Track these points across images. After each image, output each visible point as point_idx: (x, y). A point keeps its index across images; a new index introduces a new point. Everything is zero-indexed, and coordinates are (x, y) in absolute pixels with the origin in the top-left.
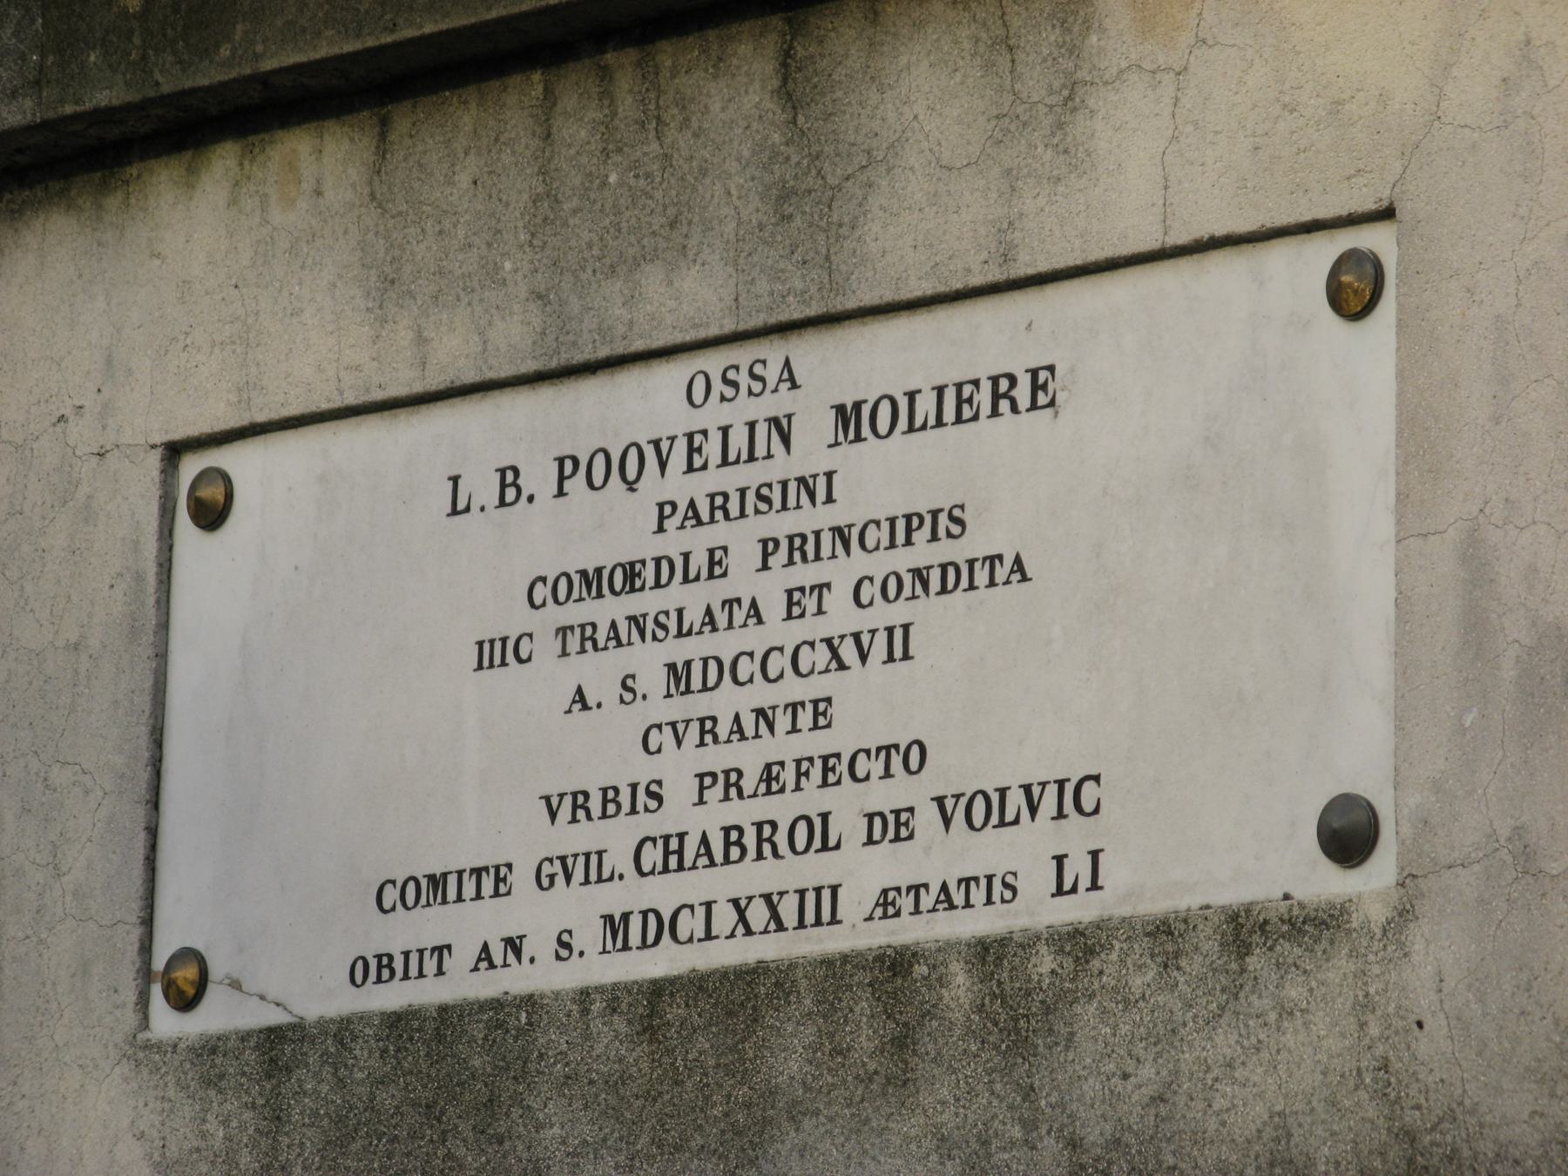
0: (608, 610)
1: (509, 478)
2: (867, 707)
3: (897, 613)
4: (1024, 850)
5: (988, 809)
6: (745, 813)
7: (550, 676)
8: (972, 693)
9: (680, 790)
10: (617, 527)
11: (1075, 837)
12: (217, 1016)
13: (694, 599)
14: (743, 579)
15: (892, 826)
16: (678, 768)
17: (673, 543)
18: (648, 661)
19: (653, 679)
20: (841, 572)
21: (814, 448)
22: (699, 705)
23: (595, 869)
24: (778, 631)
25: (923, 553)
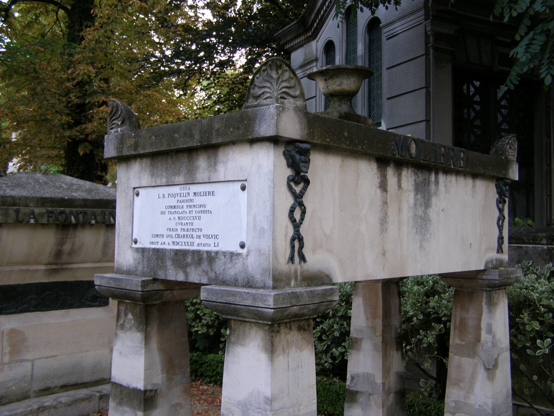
0: (173, 210)
1: (164, 195)
2: (197, 224)
3: (199, 215)
4: (211, 241)
5: (207, 237)
6: (186, 233)
7: (167, 216)
9: (179, 230)
11: (216, 241)
12: (138, 245)
14: (185, 209)
15: (199, 237)
16: (179, 227)
17: (179, 204)
18: (176, 216)
19: (177, 218)
20: (194, 210)
21: (191, 196)
22: (181, 221)
23: (171, 236)
24: (188, 215)
25: (202, 209)
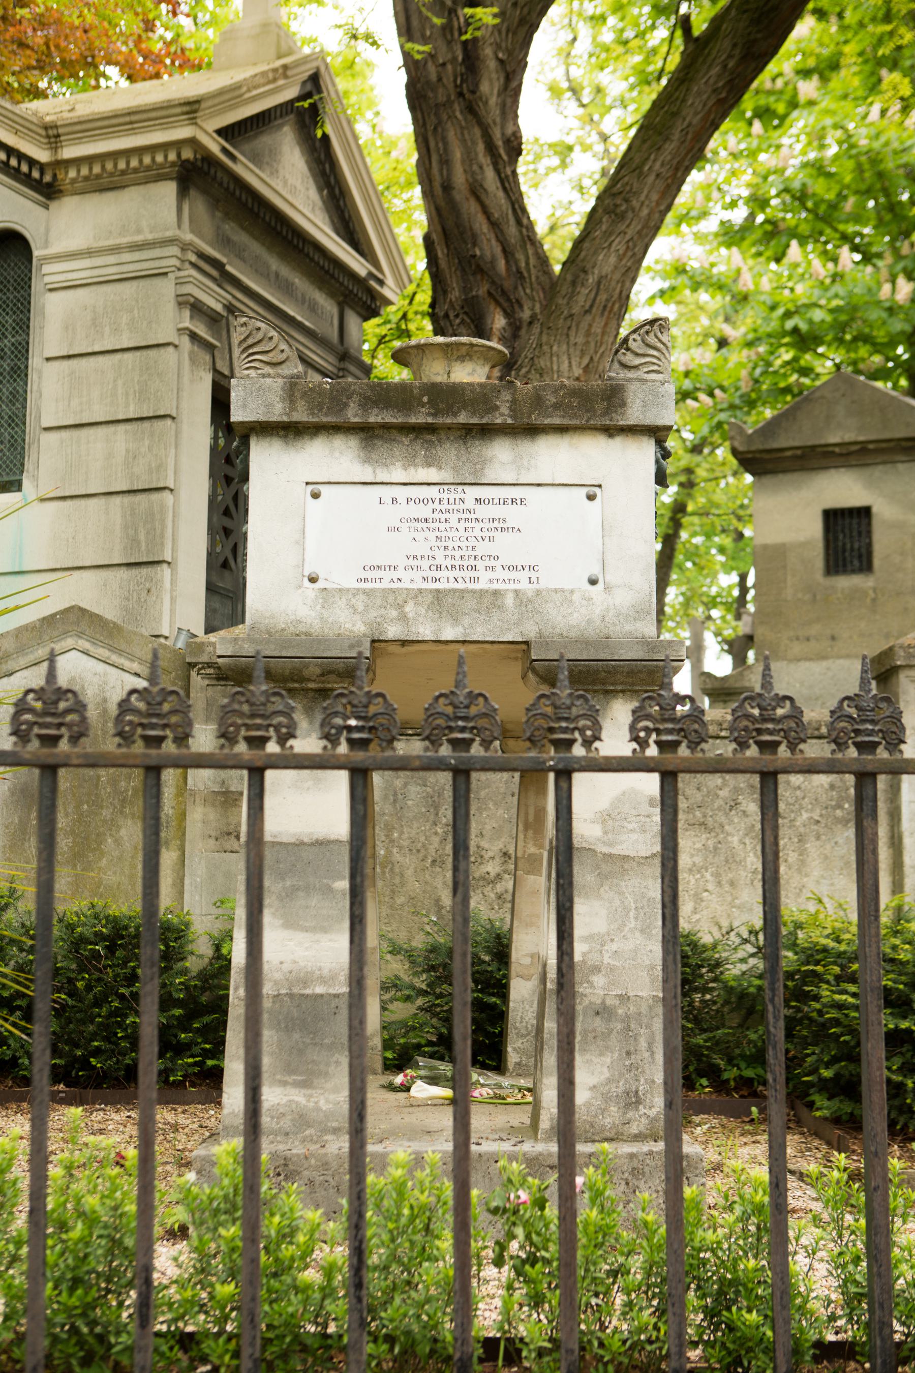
0: (420, 525)
2: (483, 548)
4: (523, 576)
8: (505, 547)
10: (424, 511)
13: (442, 526)
16: (440, 554)
17: (437, 515)
18: (432, 536)
20: (478, 526)
22: (444, 544)
25: (496, 524)
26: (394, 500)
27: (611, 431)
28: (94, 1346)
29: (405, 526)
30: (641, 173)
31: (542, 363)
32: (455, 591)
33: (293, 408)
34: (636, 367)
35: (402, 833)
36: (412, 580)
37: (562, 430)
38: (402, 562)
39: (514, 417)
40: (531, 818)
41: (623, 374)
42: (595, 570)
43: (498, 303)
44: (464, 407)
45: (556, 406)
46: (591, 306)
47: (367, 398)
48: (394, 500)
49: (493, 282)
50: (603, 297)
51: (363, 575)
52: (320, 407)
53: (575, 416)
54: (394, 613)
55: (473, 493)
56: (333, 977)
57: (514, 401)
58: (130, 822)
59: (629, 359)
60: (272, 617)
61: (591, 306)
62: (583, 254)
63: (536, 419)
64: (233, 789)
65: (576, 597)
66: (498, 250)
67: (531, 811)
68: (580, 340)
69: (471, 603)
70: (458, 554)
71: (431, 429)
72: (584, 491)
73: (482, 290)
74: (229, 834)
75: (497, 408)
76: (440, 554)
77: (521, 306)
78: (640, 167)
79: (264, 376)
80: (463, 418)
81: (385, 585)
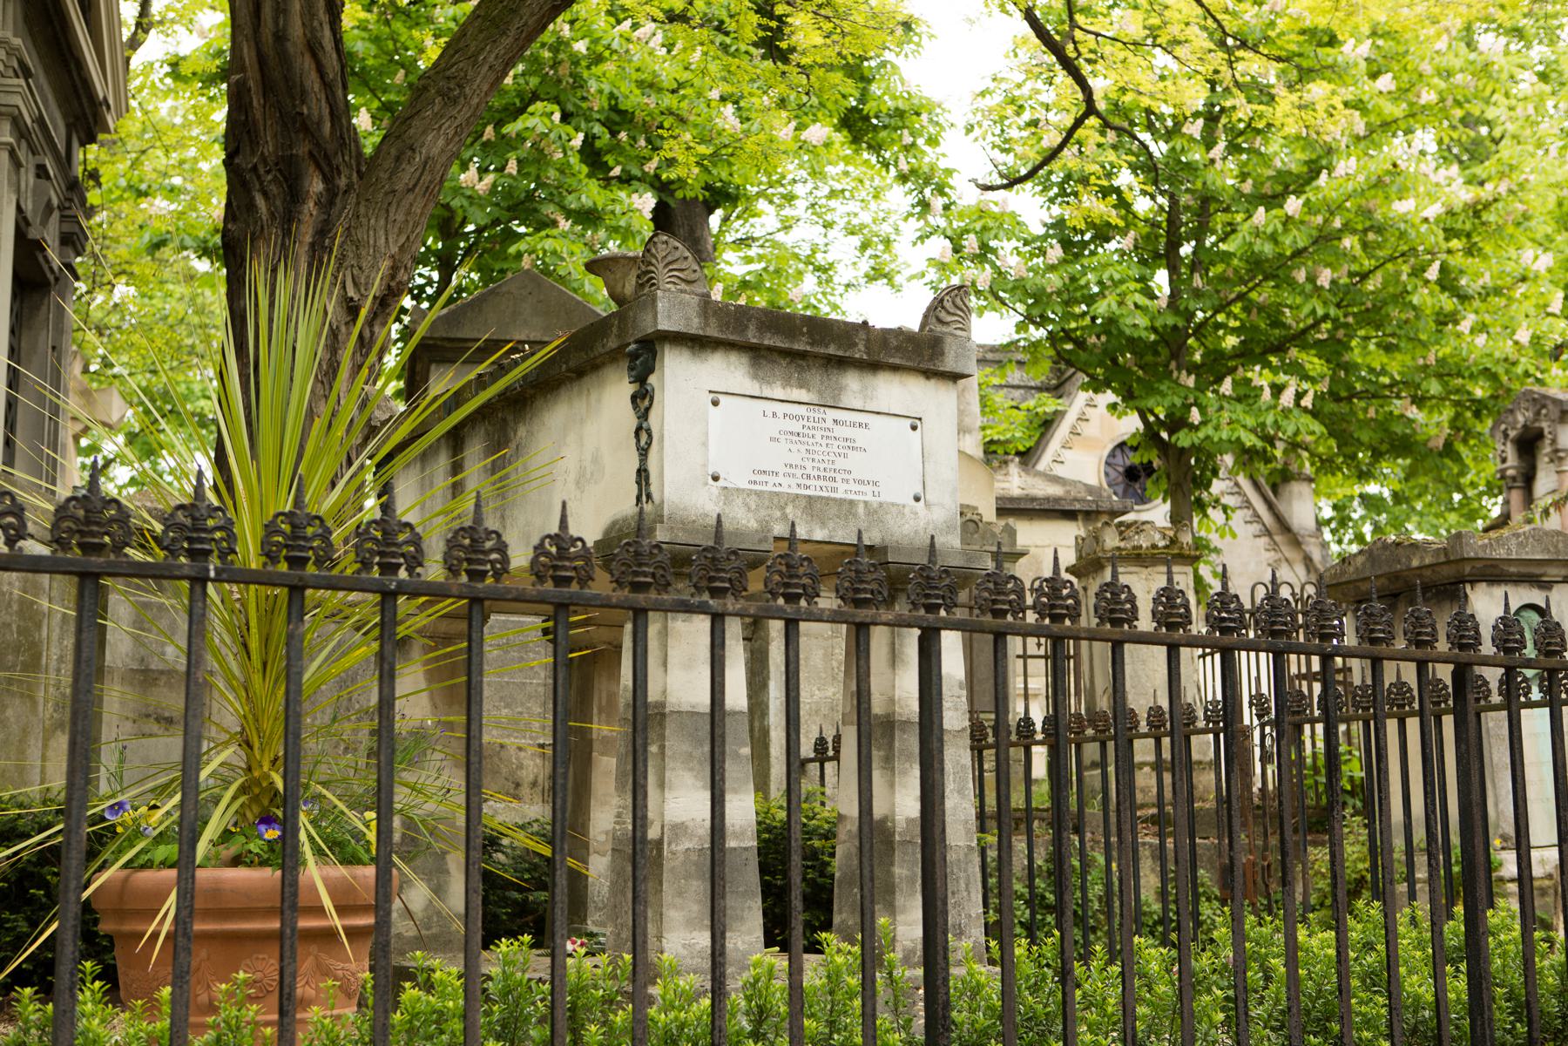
0: (795, 438)
2: (840, 463)
4: (868, 489)
5: (861, 482)
8: (854, 462)
10: (796, 426)
11: (876, 489)
13: (811, 441)
16: (809, 465)
17: (806, 431)
18: (803, 448)
20: (836, 443)
21: (829, 424)
26: (774, 414)
27: (929, 374)
28: (1561, 994)
29: (783, 437)
30: (476, 62)
31: (360, 234)
32: (822, 498)
33: (707, 324)
34: (947, 324)
35: (315, 718)
36: (789, 486)
37: (895, 368)
38: (782, 470)
39: (868, 354)
40: (604, 703)
41: (939, 328)
42: (919, 490)
43: (318, 166)
44: (833, 340)
45: (898, 349)
46: (415, 186)
47: (762, 323)
48: (774, 414)
49: (318, 145)
50: (426, 178)
51: (753, 478)
52: (727, 325)
53: (909, 359)
54: (778, 514)
55: (832, 414)
56: (743, 833)
57: (868, 340)
58: (17, 701)
59: (943, 315)
60: (685, 509)
61: (415, 186)
62: (412, 131)
63: (883, 358)
64: (153, 667)
65: (907, 511)
66: (326, 112)
67: (604, 695)
68: (400, 217)
69: (834, 510)
70: (822, 466)
71: (803, 355)
72: (909, 422)
73: (302, 149)
74: (148, 716)
75: (856, 345)
76: (809, 465)
77: (339, 173)
78: (475, 56)
79: (682, 291)
80: (832, 350)
81: (769, 488)
